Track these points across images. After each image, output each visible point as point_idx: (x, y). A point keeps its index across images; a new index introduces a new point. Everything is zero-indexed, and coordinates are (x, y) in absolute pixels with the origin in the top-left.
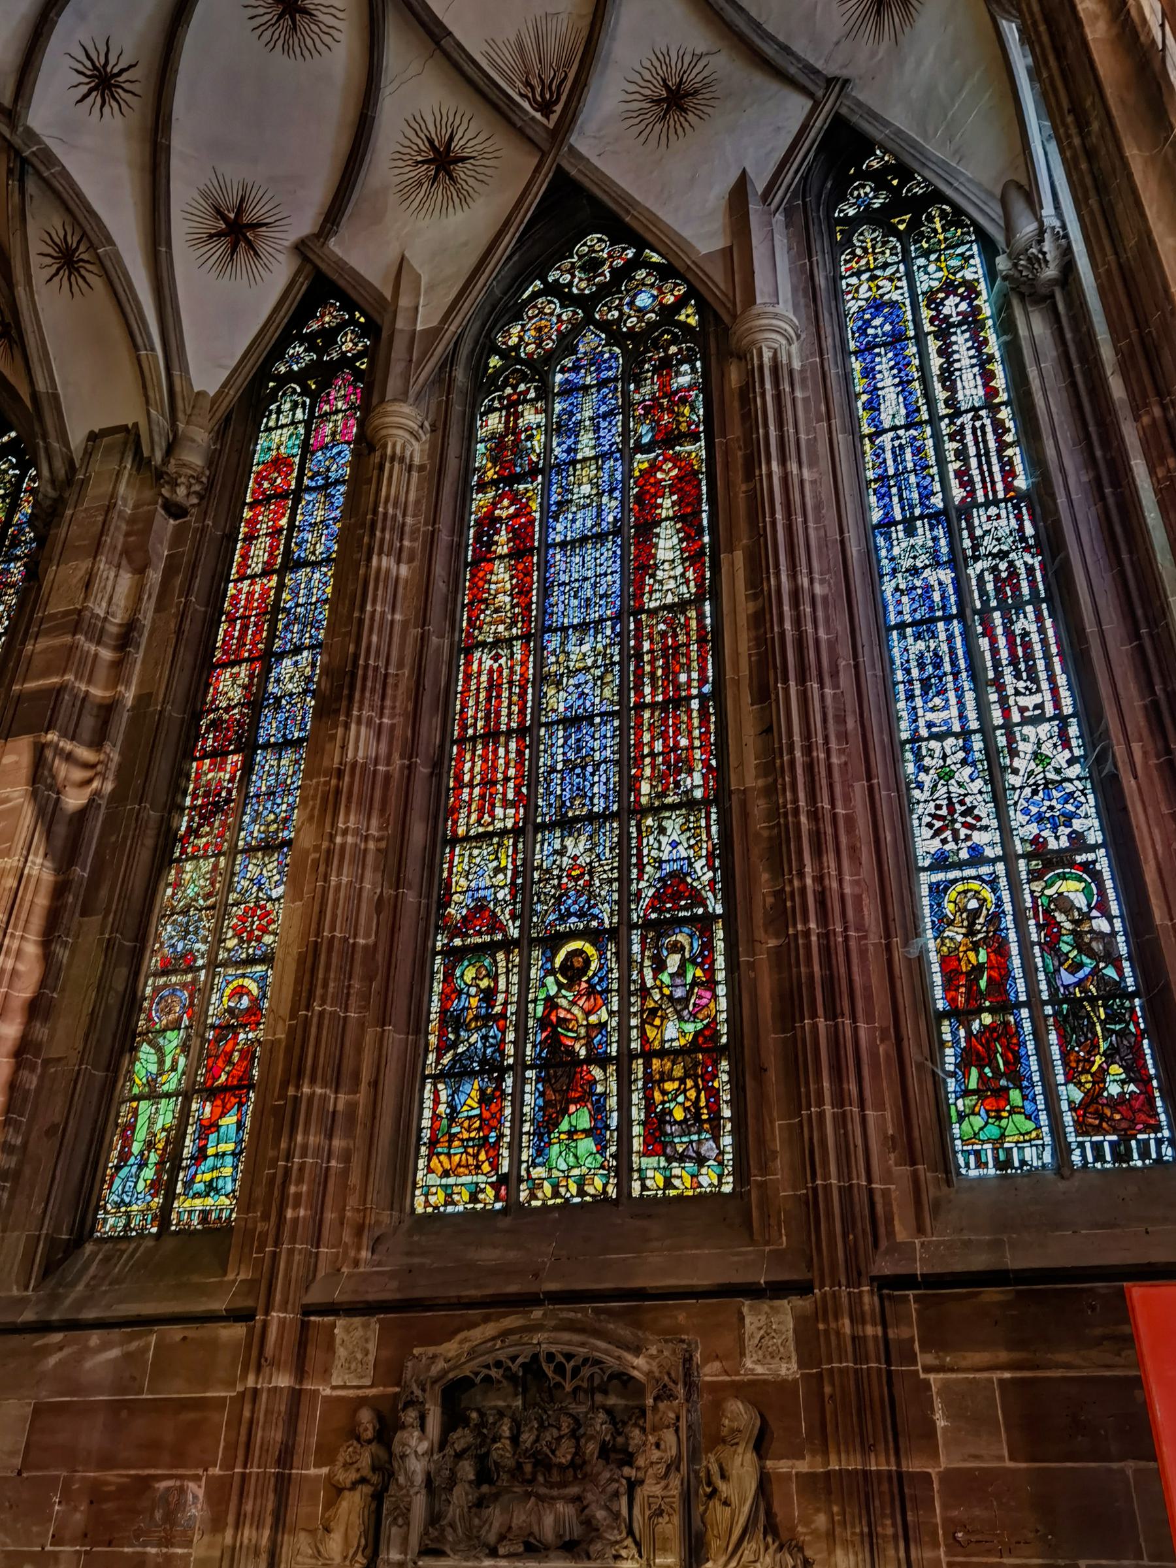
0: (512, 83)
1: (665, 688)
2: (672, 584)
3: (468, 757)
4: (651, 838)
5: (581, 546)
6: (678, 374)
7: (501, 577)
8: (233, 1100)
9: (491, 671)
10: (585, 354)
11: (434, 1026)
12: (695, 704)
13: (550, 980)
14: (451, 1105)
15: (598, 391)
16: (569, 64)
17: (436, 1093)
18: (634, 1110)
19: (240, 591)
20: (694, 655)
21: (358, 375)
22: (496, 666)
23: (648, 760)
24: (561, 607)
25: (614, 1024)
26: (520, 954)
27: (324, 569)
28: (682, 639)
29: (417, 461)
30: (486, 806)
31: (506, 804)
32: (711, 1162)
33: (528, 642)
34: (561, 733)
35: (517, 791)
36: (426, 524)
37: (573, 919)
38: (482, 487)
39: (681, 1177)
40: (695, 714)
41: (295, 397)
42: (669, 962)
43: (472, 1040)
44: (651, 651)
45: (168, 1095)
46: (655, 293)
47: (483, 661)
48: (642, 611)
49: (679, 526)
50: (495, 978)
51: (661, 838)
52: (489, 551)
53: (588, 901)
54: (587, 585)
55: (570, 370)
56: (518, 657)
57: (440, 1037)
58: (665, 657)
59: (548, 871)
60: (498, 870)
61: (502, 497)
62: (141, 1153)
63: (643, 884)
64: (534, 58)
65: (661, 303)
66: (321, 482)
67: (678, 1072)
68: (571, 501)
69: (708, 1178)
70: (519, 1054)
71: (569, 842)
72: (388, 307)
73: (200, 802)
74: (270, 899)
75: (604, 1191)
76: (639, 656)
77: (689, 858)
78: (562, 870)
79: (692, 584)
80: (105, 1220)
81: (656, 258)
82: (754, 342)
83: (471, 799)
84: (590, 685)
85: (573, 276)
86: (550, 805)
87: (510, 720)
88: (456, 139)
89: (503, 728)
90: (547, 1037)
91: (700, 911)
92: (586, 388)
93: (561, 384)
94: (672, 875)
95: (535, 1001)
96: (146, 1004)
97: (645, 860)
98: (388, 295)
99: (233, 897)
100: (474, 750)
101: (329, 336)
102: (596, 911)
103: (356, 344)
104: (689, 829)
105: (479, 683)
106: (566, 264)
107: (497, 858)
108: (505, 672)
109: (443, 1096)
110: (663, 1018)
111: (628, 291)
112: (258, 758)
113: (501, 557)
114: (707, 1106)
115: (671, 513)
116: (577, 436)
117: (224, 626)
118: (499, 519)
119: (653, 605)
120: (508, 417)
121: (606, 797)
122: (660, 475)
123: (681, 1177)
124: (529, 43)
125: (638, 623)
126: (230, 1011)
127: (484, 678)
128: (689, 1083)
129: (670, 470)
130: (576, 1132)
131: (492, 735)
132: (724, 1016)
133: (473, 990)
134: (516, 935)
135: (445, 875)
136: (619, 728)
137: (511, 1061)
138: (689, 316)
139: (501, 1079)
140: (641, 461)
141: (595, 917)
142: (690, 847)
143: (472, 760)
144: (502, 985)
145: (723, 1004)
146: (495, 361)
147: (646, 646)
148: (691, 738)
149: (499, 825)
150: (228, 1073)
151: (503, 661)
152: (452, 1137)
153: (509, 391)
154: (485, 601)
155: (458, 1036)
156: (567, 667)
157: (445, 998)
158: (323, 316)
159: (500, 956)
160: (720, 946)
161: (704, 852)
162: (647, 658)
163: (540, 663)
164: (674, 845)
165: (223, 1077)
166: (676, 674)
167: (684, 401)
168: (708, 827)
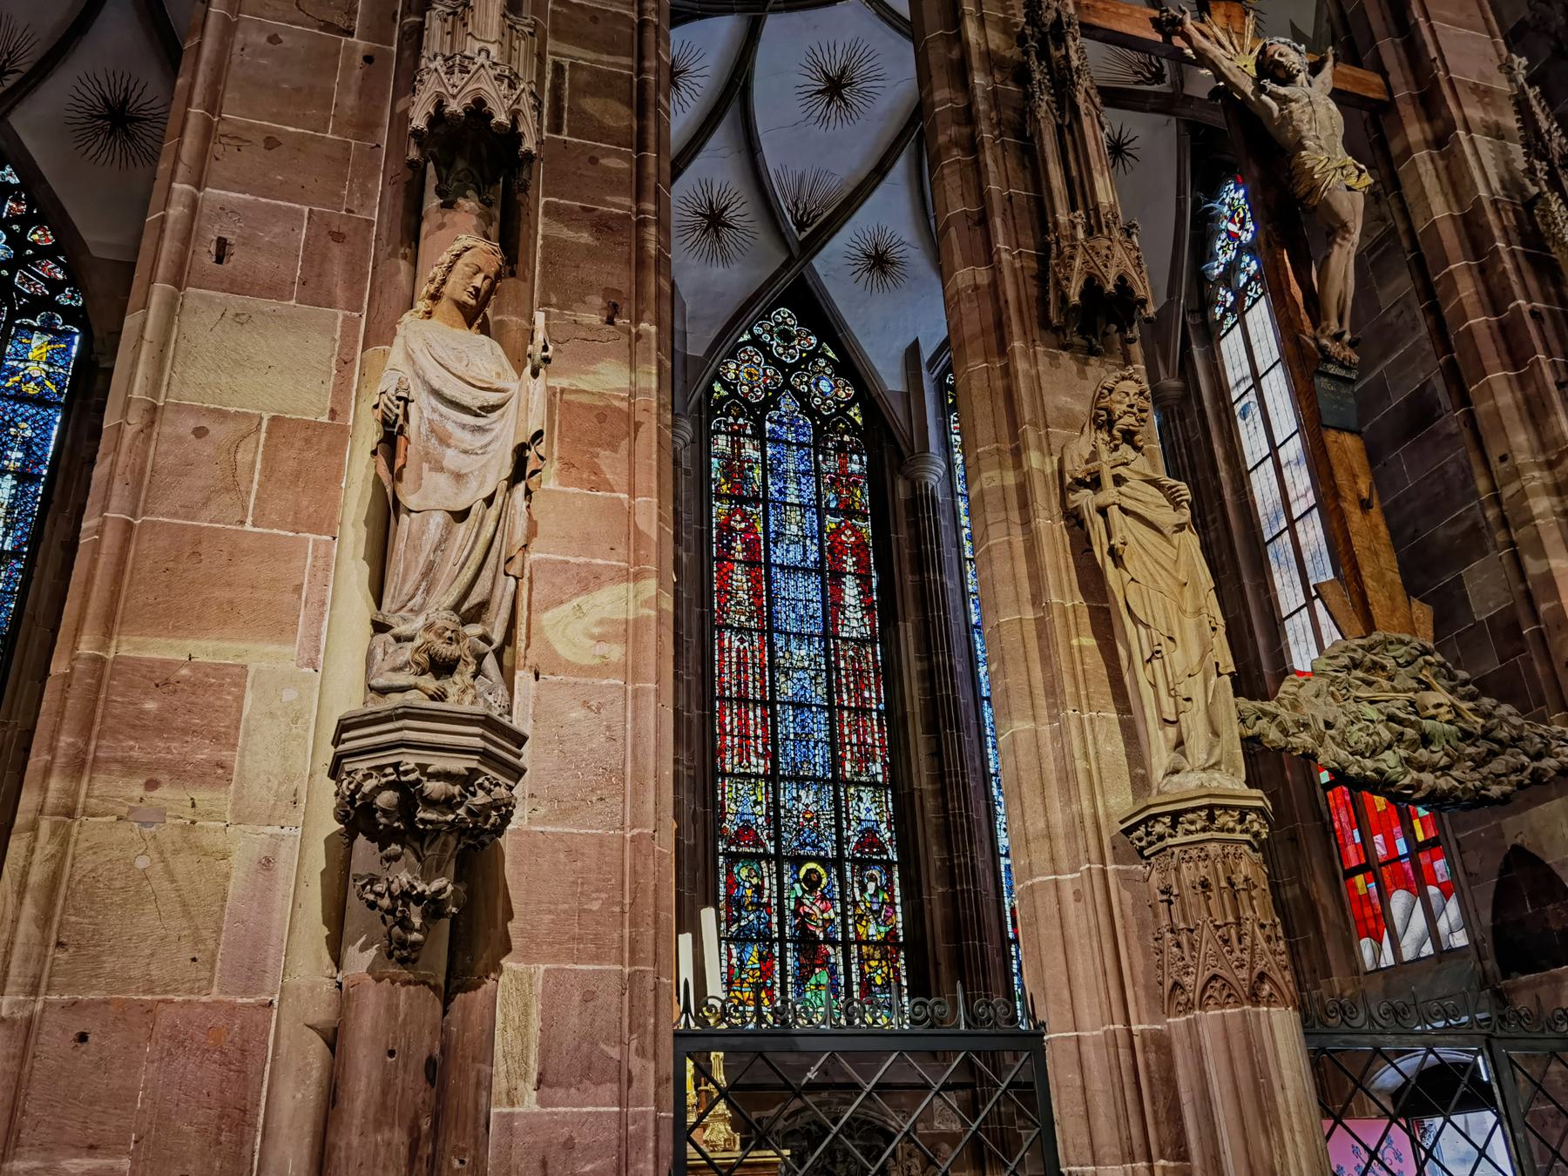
0: (784, 196)
2: (854, 623)
3: (728, 712)
7: (740, 577)
12: (874, 715)
13: (797, 886)
14: (739, 959)
16: (827, 207)
17: (729, 950)
18: (854, 976)
20: (872, 680)
23: (848, 747)
26: (776, 865)
30: (743, 752)
33: (763, 636)
34: (791, 712)
35: (765, 749)
37: (808, 848)
43: (751, 918)
50: (762, 879)
53: (817, 837)
56: (756, 644)
57: (727, 913)
58: (855, 675)
59: (790, 811)
60: (756, 803)
63: (850, 833)
64: (806, 193)
70: (781, 931)
71: (803, 793)
76: (838, 670)
81: (831, 354)
82: (924, 477)
83: (733, 746)
84: (808, 681)
92: (789, 444)
94: (868, 830)
100: (732, 710)
105: (730, 657)
108: (749, 654)
109: (734, 952)
110: (868, 921)
111: (814, 373)
113: (739, 562)
116: (785, 482)
119: (845, 635)
121: (824, 767)
122: (843, 538)
124: (808, 180)
125: (836, 644)
127: (734, 654)
128: (884, 963)
132: (900, 925)
133: (747, 885)
134: (773, 851)
135: (720, 798)
137: (776, 935)
139: (771, 947)
141: (822, 849)
144: (767, 885)
147: (842, 664)
148: (874, 739)
149: (754, 770)
151: (746, 644)
152: (743, 981)
153: (731, 420)
154: (729, 593)
155: (740, 914)
159: (764, 864)
162: (843, 673)
164: (869, 810)
166: (863, 690)
167: (856, 484)
168: (887, 802)
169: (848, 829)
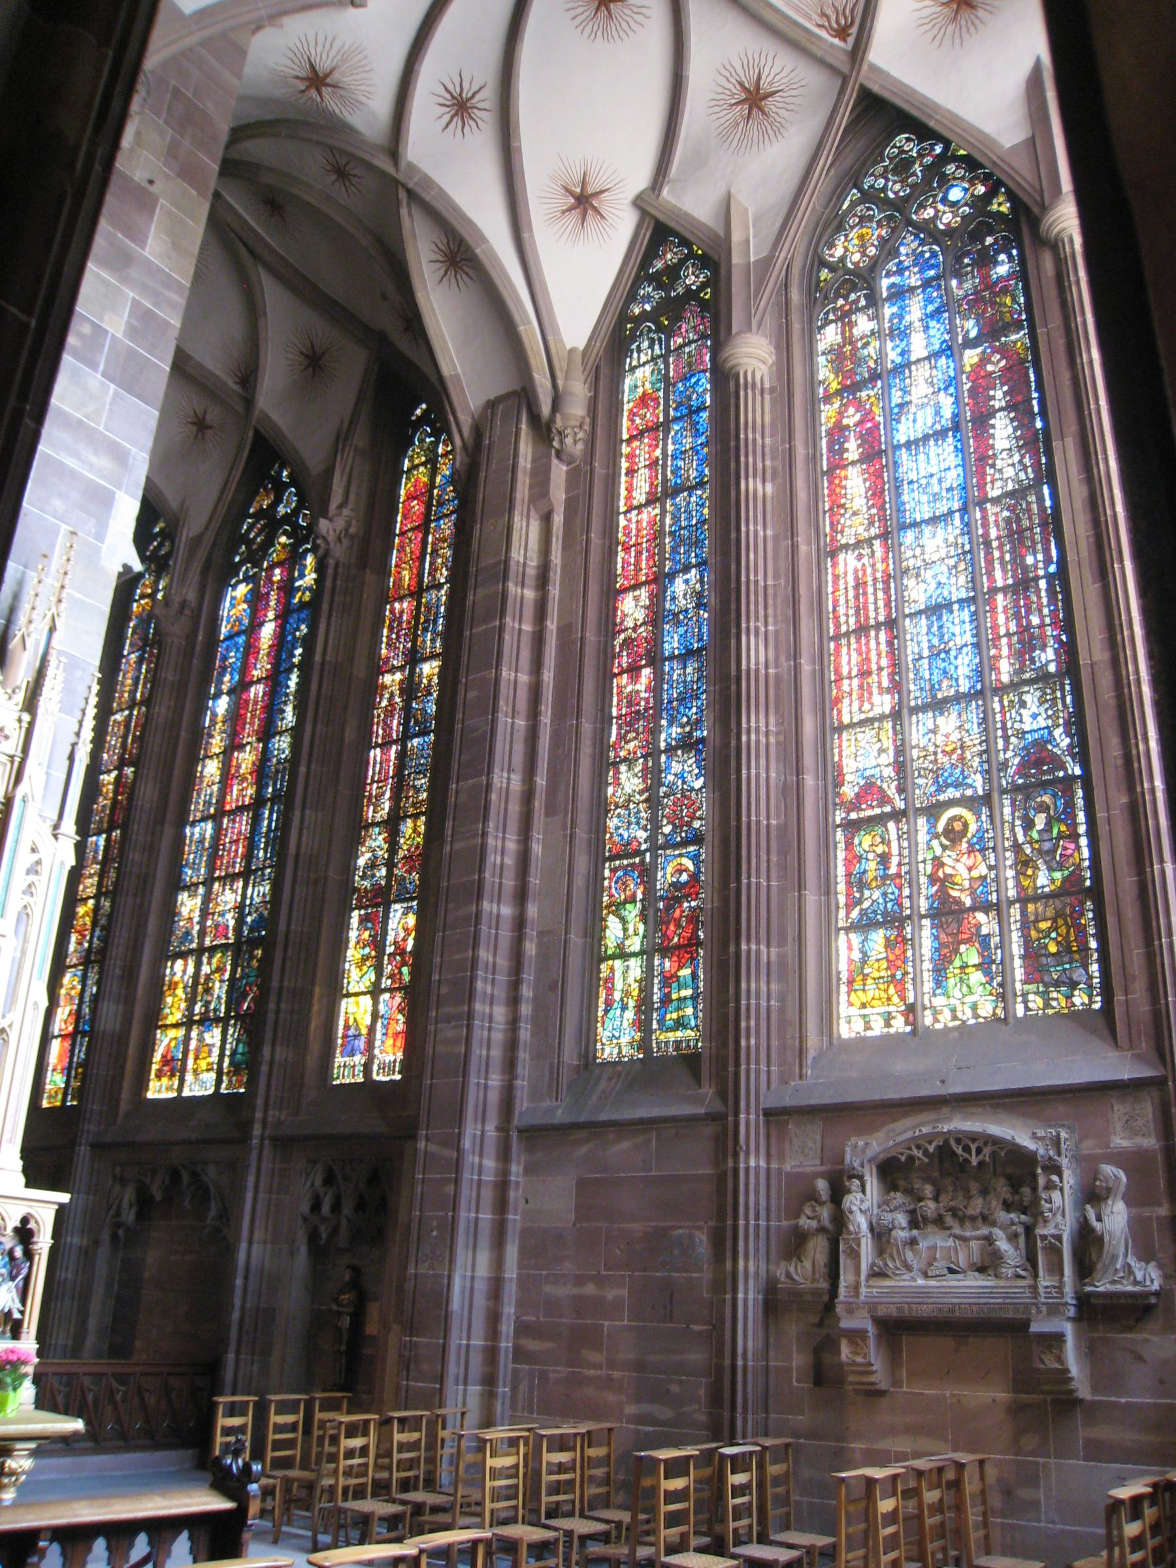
1: (1014, 571)
4: (1013, 712)
5: (924, 445)
6: (996, 263)
8: (687, 956)
9: (856, 571)
10: (907, 255)
11: (841, 887)
12: (1043, 584)
13: (935, 843)
15: (923, 292)
17: (849, 941)
19: (629, 521)
21: (703, 304)
22: (859, 566)
23: (1004, 641)
24: (913, 504)
25: (993, 876)
27: (699, 492)
28: (1026, 523)
29: (767, 385)
31: (881, 690)
32: (1082, 986)
33: (886, 540)
35: (892, 680)
36: (783, 443)
38: (828, 399)
39: (1057, 999)
40: (1043, 594)
41: (651, 335)
42: (1037, 820)
44: (999, 538)
45: (635, 955)
46: (966, 185)
47: (848, 562)
48: (987, 500)
49: (1012, 415)
50: (889, 844)
51: (1022, 711)
52: (842, 459)
53: (962, 772)
54: (934, 480)
55: (895, 273)
58: (1011, 542)
60: (881, 751)
61: (846, 406)
62: (622, 1000)
63: (1010, 754)
65: (973, 195)
66: (685, 412)
67: (1050, 913)
68: (911, 402)
69: (1080, 999)
72: (724, 243)
73: (624, 712)
74: (693, 789)
75: (994, 1014)
76: (987, 543)
77: (1048, 727)
78: (937, 746)
79: (1030, 470)
80: (603, 1050)
85: (887, 180)
86: (921, 689)
87: (877, 614)
88: (764, 77)
89: (872, 622)
90: (937, 892)
91: (1061, 774)
92: (912, 290)
93: (889, 288)
94: (1035, 743)
95: (924, 861)
96: (606, 883)
97: (1010, 732)
98: (722, 233)
99: (663, 790)
101: (673, 272)
102: (969, 781)
103: (697, 277)
104: (1046, 701)
105: (846, 583)
106: (879, 169)
107: (879, 740)
108: (869, 570)
112: (667, 669)
113: (853, 463)
114: (1075, 940)
115: (1003, 404)
117: (621, 554)
118: (847, 427)
120: (843, 326)
121: (969, 677)
122: (990, 368)
123: (1057, 999)
126: (673, 885)
128: (1060, 922)
129: (999, 361)
130: (967, 966)
131: (862, 630)
132: (1087, 863)
134: (903, 807)
136: (975, 613)
137: (908, 912)
138: (1001, 206)
140: (971, 357)
141: (971, 786)
142: (1048, 717)
143: (849, 654)
144: (895, 850)
145: (1086, 853)
146: (825, 274)
147: (993, 533)
148: (1042, 617)
150: (679, 935)
151: (865, 560)
153: (841, 302)
155: (862, 894)
156: (924, 560)
157: (848, 863)
158: (664, 254)
160: (1080, 803)
161: (1061, 721)
162: (995, 544)
163: (898, 560)
164: (1035, 716)
165: (676, 939)
166: (1023, 558)
167: (1005, 291)
168: (1063, 698)
169: (1006, 750)
